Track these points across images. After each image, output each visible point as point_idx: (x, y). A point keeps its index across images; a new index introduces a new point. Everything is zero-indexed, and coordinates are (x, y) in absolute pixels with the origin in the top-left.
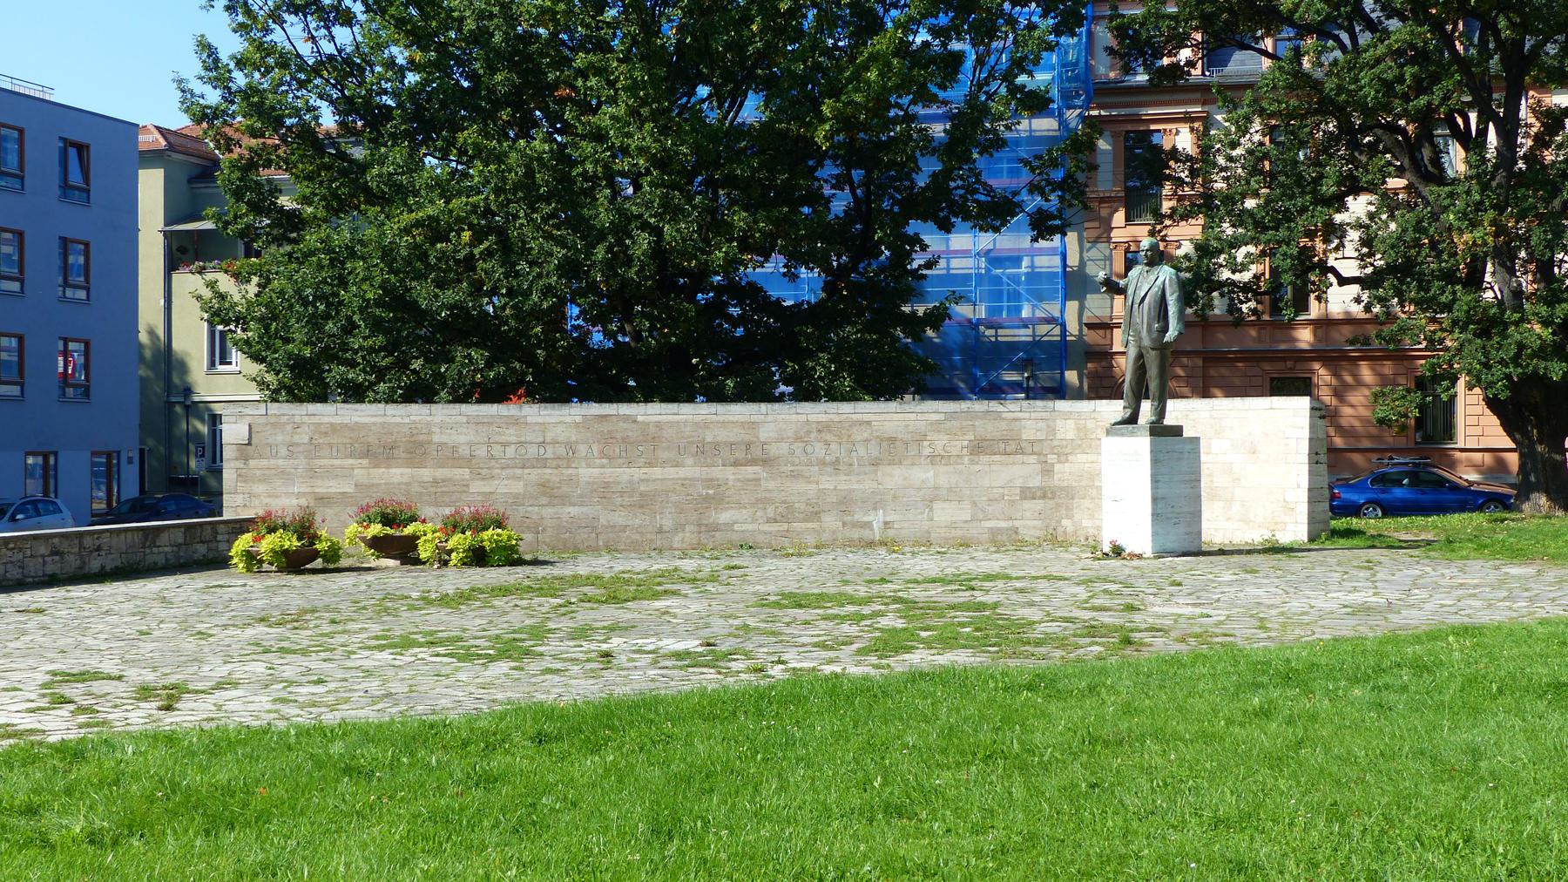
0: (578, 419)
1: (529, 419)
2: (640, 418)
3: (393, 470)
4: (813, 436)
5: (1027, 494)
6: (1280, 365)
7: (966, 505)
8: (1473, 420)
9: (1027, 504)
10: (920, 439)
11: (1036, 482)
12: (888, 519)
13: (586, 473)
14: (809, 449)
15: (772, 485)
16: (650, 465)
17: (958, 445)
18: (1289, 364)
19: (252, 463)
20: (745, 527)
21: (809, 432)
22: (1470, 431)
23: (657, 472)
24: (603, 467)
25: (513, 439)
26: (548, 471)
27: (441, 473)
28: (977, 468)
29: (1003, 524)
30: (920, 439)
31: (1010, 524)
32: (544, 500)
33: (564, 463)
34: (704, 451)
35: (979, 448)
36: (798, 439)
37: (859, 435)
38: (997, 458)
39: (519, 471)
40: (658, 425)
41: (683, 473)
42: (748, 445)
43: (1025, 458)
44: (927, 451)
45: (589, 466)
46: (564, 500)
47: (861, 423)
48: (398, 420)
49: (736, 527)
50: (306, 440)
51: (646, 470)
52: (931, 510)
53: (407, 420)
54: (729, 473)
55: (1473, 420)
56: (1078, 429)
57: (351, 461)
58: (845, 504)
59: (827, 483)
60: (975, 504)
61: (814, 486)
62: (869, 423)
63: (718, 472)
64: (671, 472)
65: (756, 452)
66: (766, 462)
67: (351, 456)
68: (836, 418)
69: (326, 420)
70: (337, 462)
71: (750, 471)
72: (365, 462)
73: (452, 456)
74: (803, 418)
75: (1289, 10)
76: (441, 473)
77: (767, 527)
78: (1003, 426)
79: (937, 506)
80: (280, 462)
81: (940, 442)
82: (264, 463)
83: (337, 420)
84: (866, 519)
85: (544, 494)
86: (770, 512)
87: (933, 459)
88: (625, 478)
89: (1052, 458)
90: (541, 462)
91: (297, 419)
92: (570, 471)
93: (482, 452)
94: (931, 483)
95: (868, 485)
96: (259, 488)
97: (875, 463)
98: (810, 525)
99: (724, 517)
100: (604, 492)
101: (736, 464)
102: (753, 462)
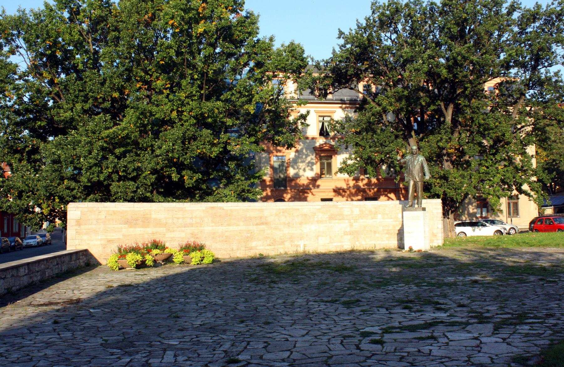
0: (204, 208)
1: (187, 209)
2: (225, 208)
3: (137, 229)
4: (281, 214)
5: (346, 233)
11: (348, 229)
12: (305, 243)
13: (207, 229)
16: (228, 225)
19: (82, 227)
21: (280, 213)
23: (231, 228)
24: (212, 226)
26: (193, 228)
27: (155, 230)
29: (339, 244)
35: (332, 218)
36: (277, 215)
38: (337, 221)
39: (183, 229)
40: (231, 211)
42: (261, 218)
44: (316, 219)
48: (139, 209)
50: (103, 217)
51: (227, 227)
52: (318, 240)
53: (142, 209)
56: (360, 211)
57: (122, 226)
60: (330, 237)
62: (298, 209)
63: (251, 228)
66: (266, 224)
67: (120, 224)
68: (288, 208)
69: (111, 209)
70: (116, 226)
72: (126, 226)
73: (158, 223)
76: (155, 230)
77: (268, 248)
79: (319, 238)
80: (94, 226)
82: (87, 227)
83: (116, 209)
84: (298, 243)
86: (268, 242)
87: (318, 222)
89: (352, 221)
90: (191, 225)
91: (100, 209)
93: (170, 221)
96: (85, 237)
97: (301, 224)
98: (281, 246)
99: (254, 244)
101: (257, 224)
102: (262, 224)
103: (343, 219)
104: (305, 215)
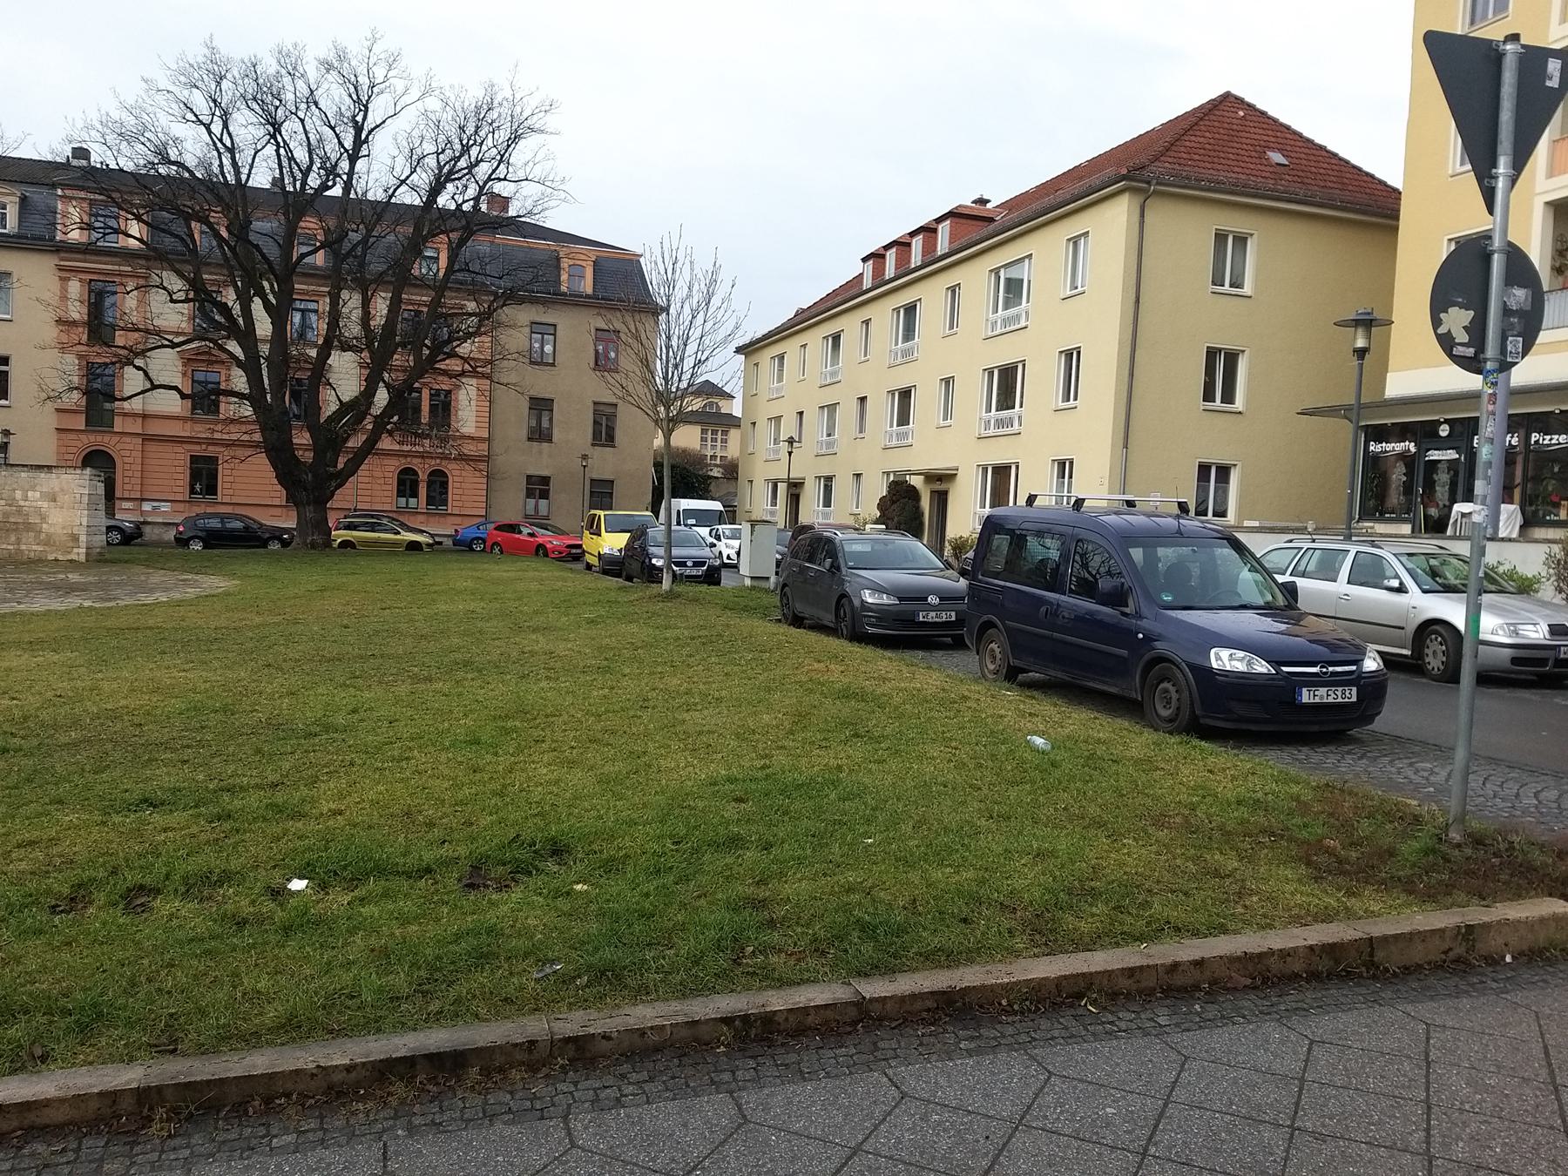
6: (197, 447)
18: (204, 447)
75: (275, 182)
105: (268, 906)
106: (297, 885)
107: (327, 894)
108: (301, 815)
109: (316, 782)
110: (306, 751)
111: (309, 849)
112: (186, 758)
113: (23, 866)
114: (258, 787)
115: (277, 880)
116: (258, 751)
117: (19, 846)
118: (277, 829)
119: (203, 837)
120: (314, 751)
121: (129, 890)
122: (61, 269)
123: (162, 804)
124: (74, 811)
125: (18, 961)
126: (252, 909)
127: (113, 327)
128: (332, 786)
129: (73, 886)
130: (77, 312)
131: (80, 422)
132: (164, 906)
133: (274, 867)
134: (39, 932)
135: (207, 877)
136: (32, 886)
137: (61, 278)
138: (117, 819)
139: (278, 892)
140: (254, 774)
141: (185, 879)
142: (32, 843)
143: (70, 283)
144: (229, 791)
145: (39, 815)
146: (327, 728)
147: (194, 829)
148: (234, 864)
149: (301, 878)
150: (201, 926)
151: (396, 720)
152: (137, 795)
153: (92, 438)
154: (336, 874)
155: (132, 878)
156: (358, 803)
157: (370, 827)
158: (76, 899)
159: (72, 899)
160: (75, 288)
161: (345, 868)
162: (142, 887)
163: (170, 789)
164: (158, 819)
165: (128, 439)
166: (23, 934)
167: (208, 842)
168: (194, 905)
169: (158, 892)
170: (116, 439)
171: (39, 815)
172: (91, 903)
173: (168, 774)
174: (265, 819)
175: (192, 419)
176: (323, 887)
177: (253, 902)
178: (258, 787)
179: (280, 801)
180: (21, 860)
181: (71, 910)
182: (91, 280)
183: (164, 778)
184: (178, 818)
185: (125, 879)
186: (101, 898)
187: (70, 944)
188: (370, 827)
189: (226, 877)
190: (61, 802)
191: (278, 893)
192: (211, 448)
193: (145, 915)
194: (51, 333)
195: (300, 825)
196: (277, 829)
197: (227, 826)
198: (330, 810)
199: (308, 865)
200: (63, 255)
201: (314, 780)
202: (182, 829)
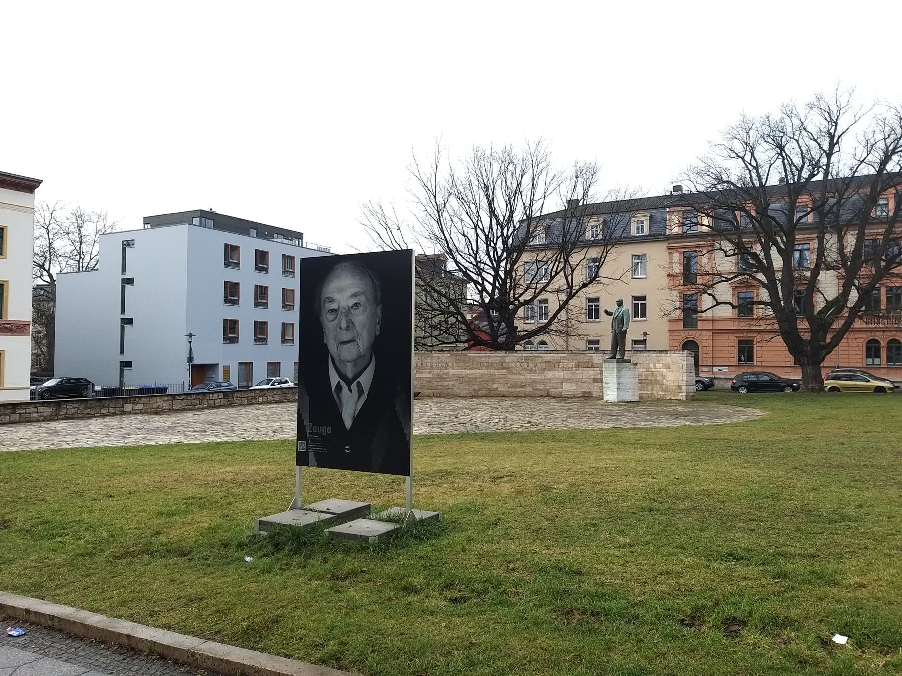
6: (742, 335)
7: (574, 383)
8: (760, 356)
9: (596, 384)
10: (558, 362)
14: (522, 365)
15: (509, 376)
17: (571, 364)
18: (745, 334)
20: (501, 389)
22: (758, 359)
23: (473, 371)
25: (429, 361)
28: (578, 372)
30: (558, 362)
31: (589, 390)
32: (438, 380)
33: (444, 368)
34: (488, 366)
35: (578, 365)
37: (538, 360)
38: (585, 368)
41: (481, 371)
43: (595, 369)
44: (561, 366)
45: (452, 369)
46: (444, 379)
47: (539, 357)
49: (498, 389)
54: (496, 372)
55: (760, 356)
58: (534, 382)
59: (528, 376)
61: (523, 377)
62: (541, 357)
63: (492, 372)
64: (478, 371)
65: (505, 365)
66: (507, 368)
68: (531, 355)
71: (504, 371)
74: (520, 355)
75: (781, 180)
78: (587, 358)
81: (565, 363)
85: (438, 378)
88: (464, 373)
92: (446, 371)
94: (562, 377)
95: (541, 377)
97: (544, 370)
98: (522, 389)
100: (458, 378)
101: (498, 369)
102: (504, 369)
103: (593, 366)
104: (548, 362)
105: (821, 653)
106: (840, 640)
107: (864, 652)
108: (836, 584)
109: (841, 558)
110: (831, 534)
111: (845, 612)
112: (752, 528)
113: (664, 588)
114: (802, 556)
115: (825, 634)
116: (798, 529)
117: (661, 574)
118: (819, 592)
119: (770, 589)
120: (837, 534)
121: (727, 620)
122: (669, 249)
123: (742, 559)
124: (690, 555)
125: (664, 656)
126: (809, 653)
127: (696, 274)
128: (854, 564)
129: (692, 609)
130: (678, 269)
131: (680, 326)
132: (751, 636)
133: (821, 621)
134: (675, 638)
135: (776, 620)
136: (669, 603)
137: (670, 253)
138: (715, 565)
139: (826, 642)
140: (798, 545)
141: (762, 619)
142: (668, 573)
143: (674, 255)
144: (782, 556)
145: (671, 555)
146: (843, 518)
147: (764, 582)
148: (793, 613)
149: (842, 634)
150: (775, 657)
151: (894, 517)
152: (725, 551)
153: (686, 334)
154: (869, 637)
155: (729, 611)
156: (877, 580)
157: (891, 603)
158: (694, 619)
159: (693, 618)
160: (676, 257)
161: (876, 634)
162: (734, 619)
163: (745, 549)
164: (740, 570)
165: (705, 333)
166: (667, 637)
167: (774, 593)
168: (769, 639)
169: (745, 624)
170: (698, 334)
171: (671, 555)
172: (704, 622)
173: (743, 537)
174: (810, 583)
175: (738, 320)
176: (860, 645)
177: (809, 648)
178: (802, 556)
179: (818, 569)
180: (663, 584)
181: (693, 625)
182: (684, 252)
183: (742, 541)
184: (753, 571)
185: (724, 611)
186: (710, 621)
187: (693, 651)
188: (891, 603)
189: (788, 623)
190: (682, 548)
191: (826, 643)
192: (749, 335)
193: (737, 640)
194: (665, 281)
195: (835, 591)
196: (819, 592)
197: (786, 583)
198: (856, 583)
199: (847, 625)
200: (670, 241)
201: (840, 557)
202: (755, 580)
